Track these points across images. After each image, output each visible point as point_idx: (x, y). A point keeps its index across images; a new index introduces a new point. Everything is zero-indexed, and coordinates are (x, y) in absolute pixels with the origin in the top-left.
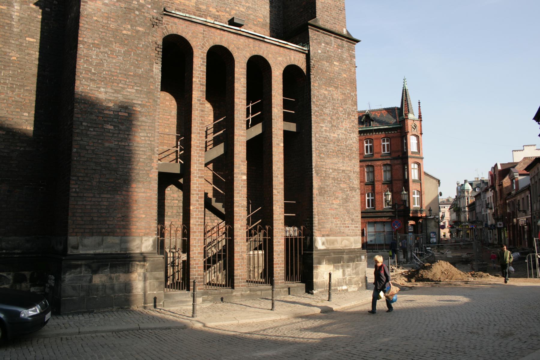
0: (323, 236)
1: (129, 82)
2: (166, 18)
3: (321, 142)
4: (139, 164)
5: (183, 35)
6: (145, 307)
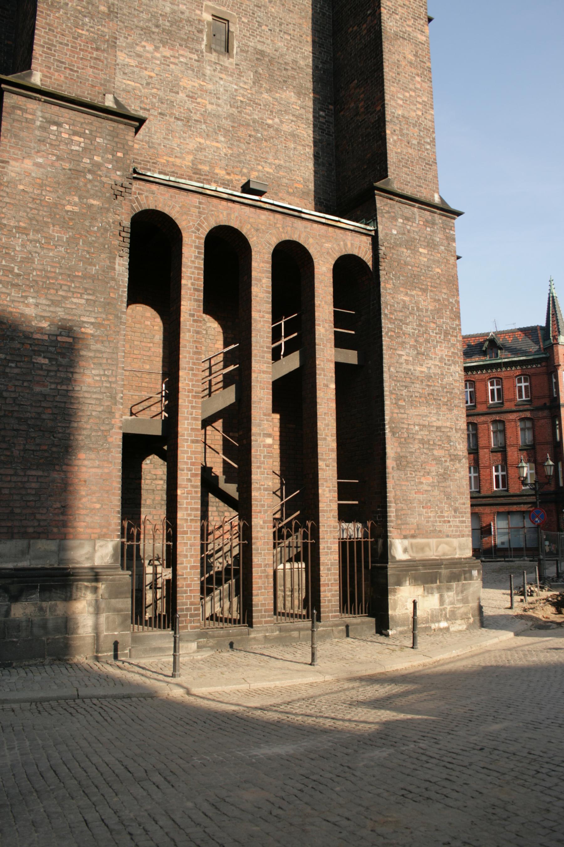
0: (405, 537)
1: (76, 287)
2: (137, 185)
3: (399, 381)
4: (91, 421)
5: (166, 211)
6: (97, 659)
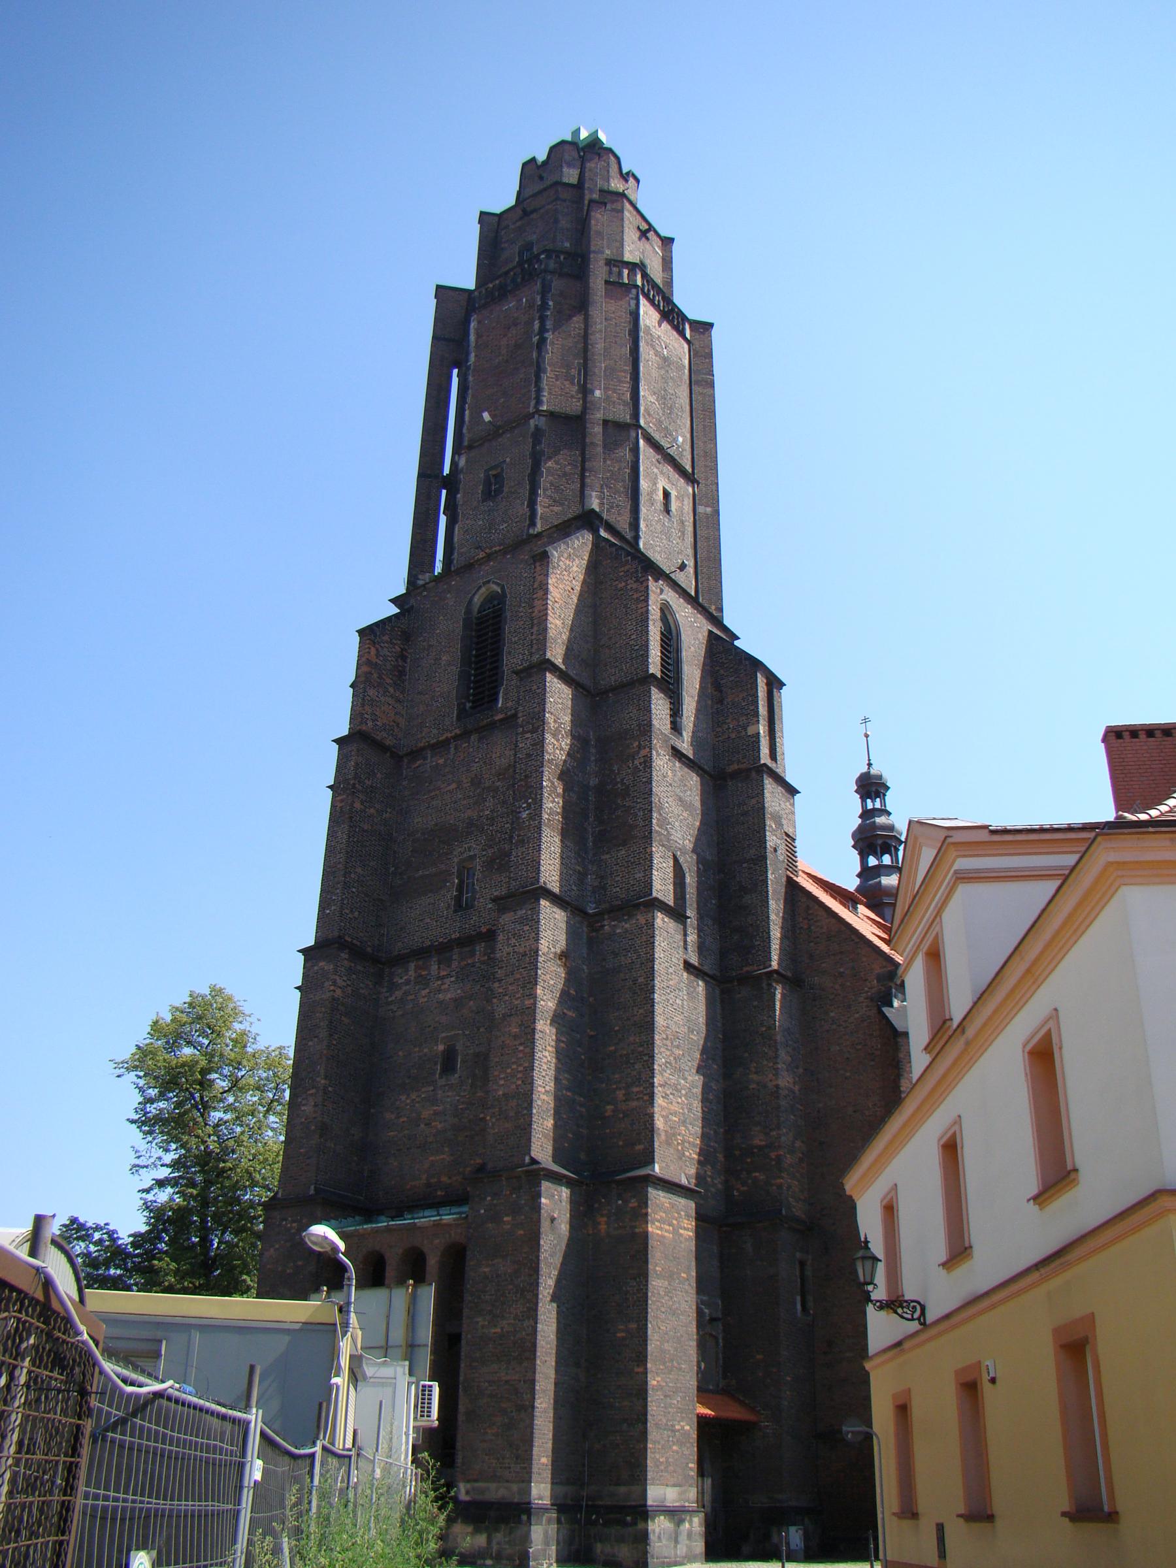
0: (468, 1481)
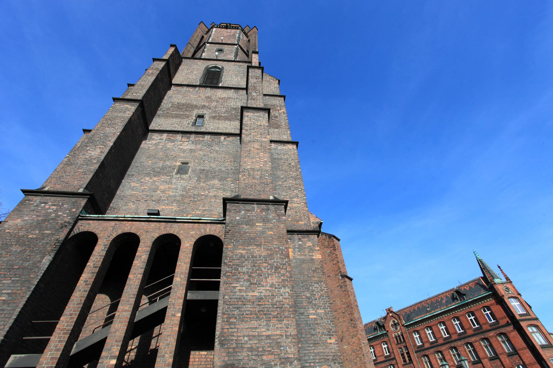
3: (232, 305)
5: (93, 231)
